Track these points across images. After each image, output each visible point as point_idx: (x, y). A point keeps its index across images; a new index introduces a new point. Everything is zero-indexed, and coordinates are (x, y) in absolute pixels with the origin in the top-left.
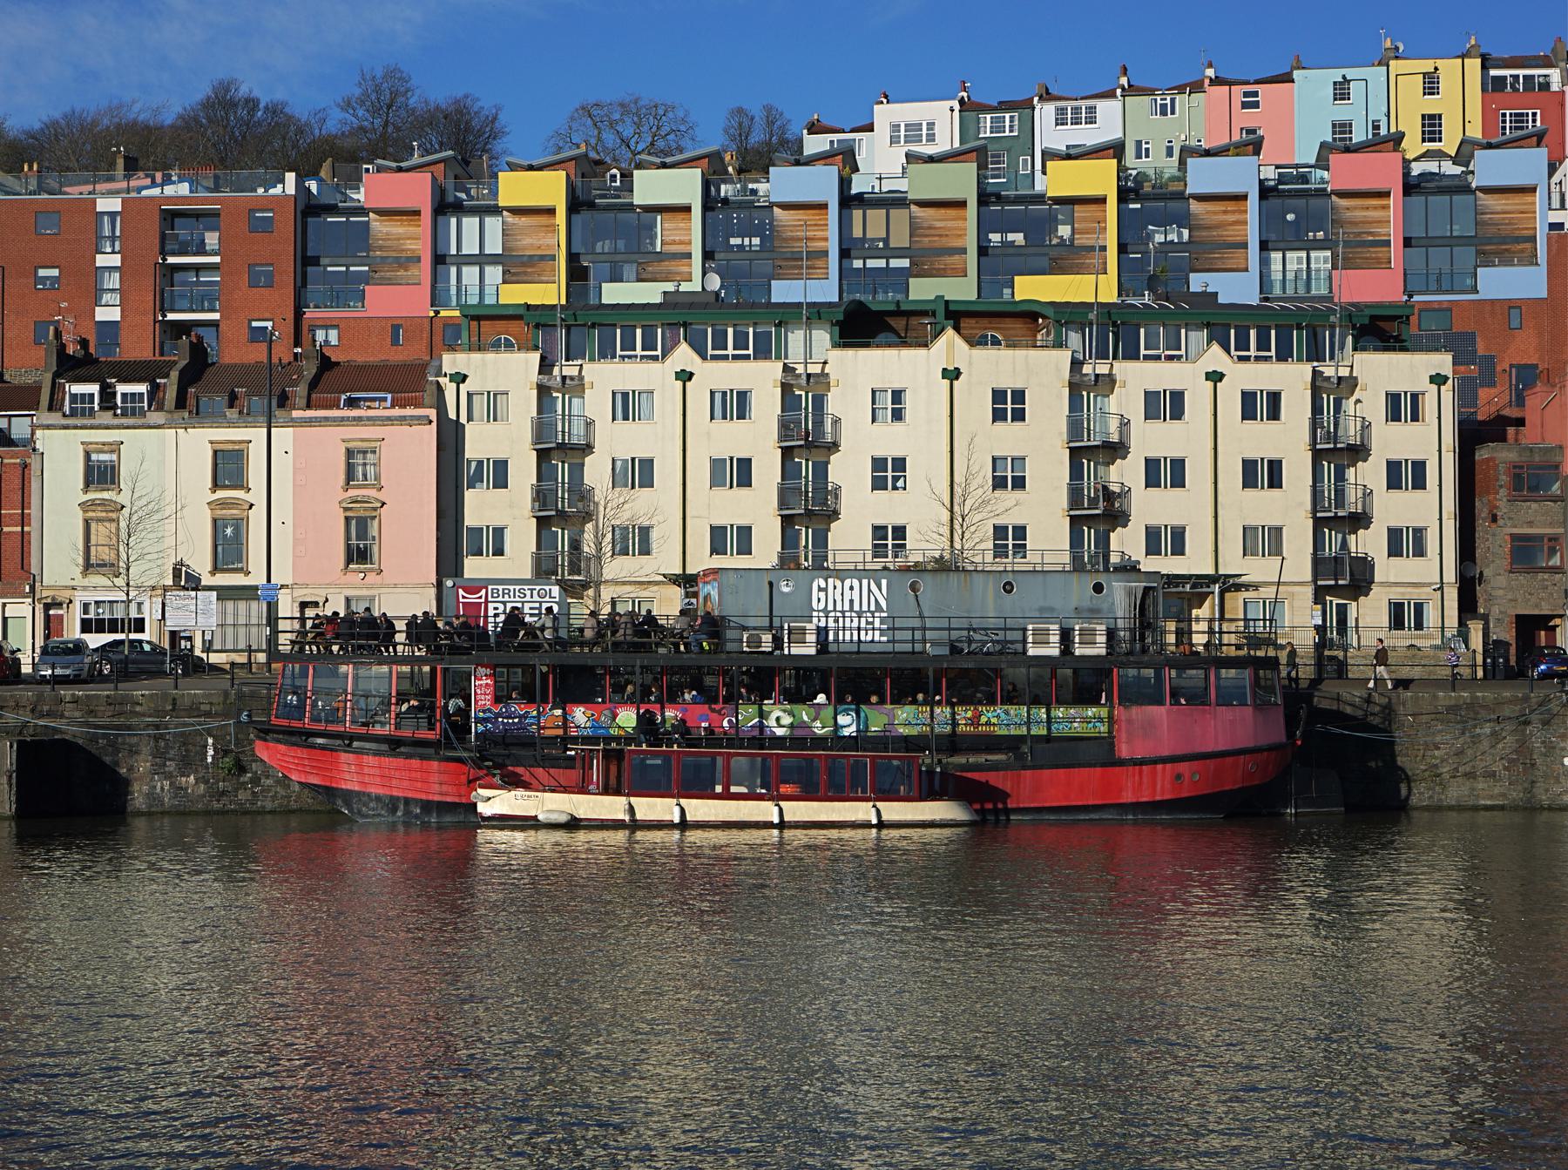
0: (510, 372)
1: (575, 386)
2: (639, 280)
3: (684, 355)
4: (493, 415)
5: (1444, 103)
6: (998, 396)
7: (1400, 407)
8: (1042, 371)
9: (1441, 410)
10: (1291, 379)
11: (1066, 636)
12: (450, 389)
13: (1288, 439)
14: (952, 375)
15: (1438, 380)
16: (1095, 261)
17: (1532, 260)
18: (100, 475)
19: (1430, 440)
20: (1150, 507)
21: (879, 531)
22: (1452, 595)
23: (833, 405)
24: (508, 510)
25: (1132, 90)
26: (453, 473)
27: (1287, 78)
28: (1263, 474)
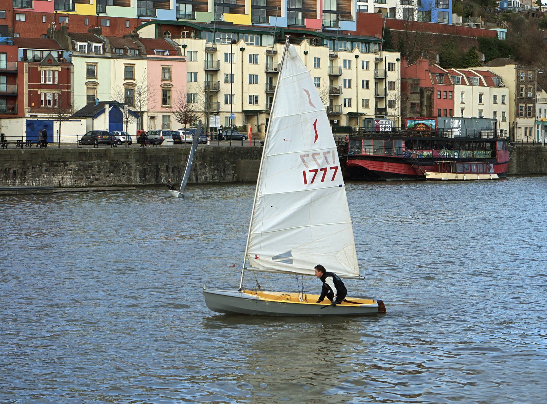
0: (197, 45)
2: (114, 5)
12: (182, 49)
14: (306, 53)
16: (241, 9)
18: (91, 73)
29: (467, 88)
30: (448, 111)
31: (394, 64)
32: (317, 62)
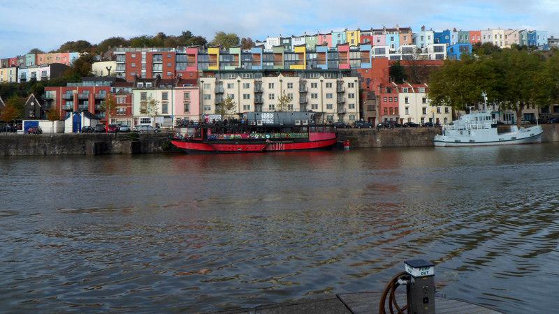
0: (211, 81)
1: (221, 83)
3: (239, 78)
4: (208, 88)
5: (355, 38)
6: (288, 84)
7: (351, 85)
8: (295, 80)
9: (356, 86)
10: (334, 81)
11: (301, 122)
13: (333, 90)
14: (281, 81)
15: (356, 81)
17: (369, 62)
18: (143, 96)
19: (355, 91)
20: (312, 101)
21: (270, 106)
22: (359, 114)
23: (263, 86)
24: (211, 103)
25: (307, 36)
26: (202, 98)
27: (331, 34)
28: (329, 96)
29: (411, 96)
30: (394, 110)
31: (353, 84)
32: (290, 86)
